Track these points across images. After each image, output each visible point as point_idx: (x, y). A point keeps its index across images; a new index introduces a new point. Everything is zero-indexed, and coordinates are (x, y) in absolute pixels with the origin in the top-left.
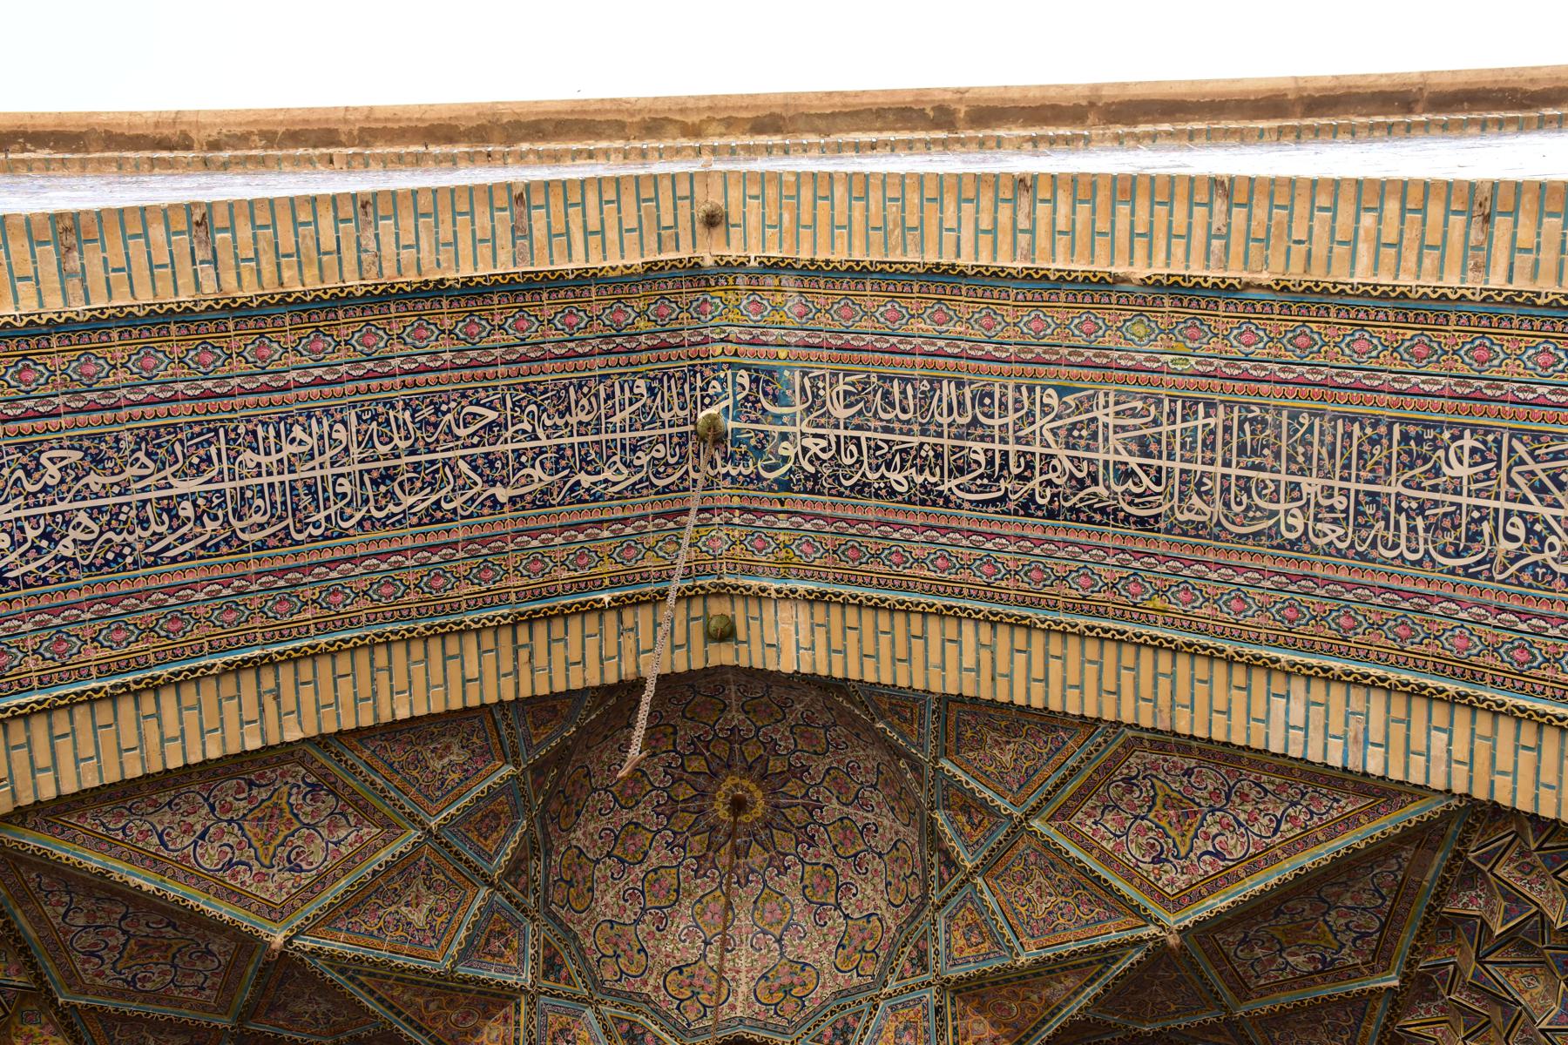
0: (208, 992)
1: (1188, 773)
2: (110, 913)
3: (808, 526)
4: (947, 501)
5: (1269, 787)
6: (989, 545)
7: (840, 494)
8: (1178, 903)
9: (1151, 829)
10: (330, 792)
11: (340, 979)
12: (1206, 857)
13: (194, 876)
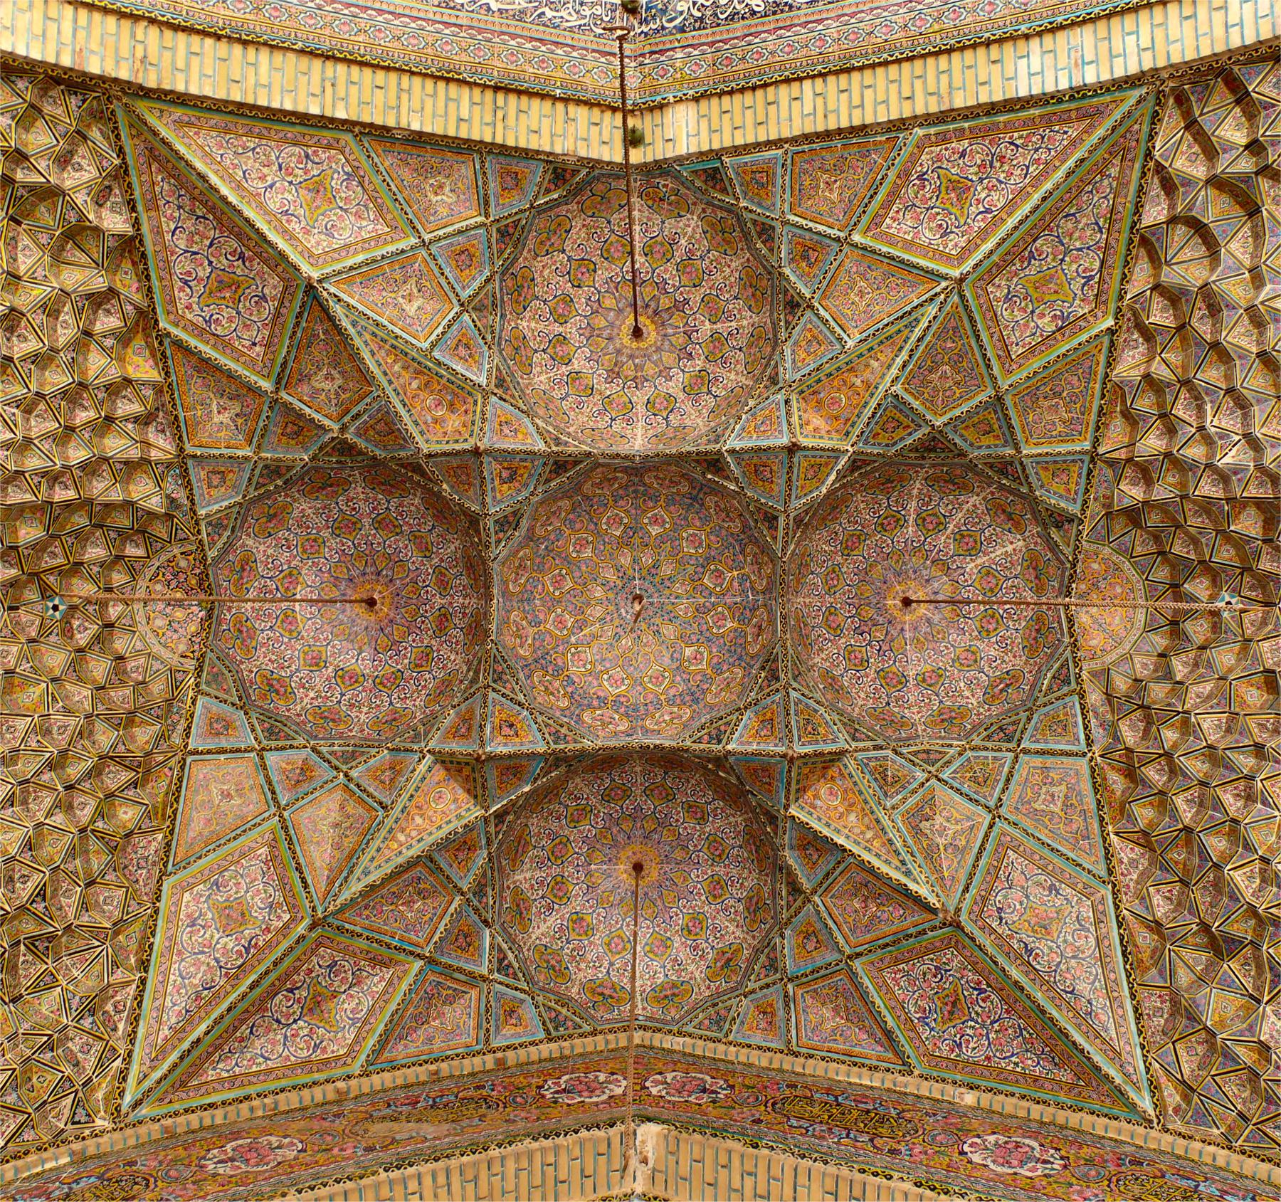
0: (258, 348)
1: (963, 155)
2: (203, 237)
3: (696, 52)
4: (791, 7)
5: (1019, 142)
6: (820, 27)
7: (718, 25)
8: (961, 258)
9: (938, 214)
10: (361, 184)
11: (352, 331)
12: (980, 217)
13: (261, 207)
